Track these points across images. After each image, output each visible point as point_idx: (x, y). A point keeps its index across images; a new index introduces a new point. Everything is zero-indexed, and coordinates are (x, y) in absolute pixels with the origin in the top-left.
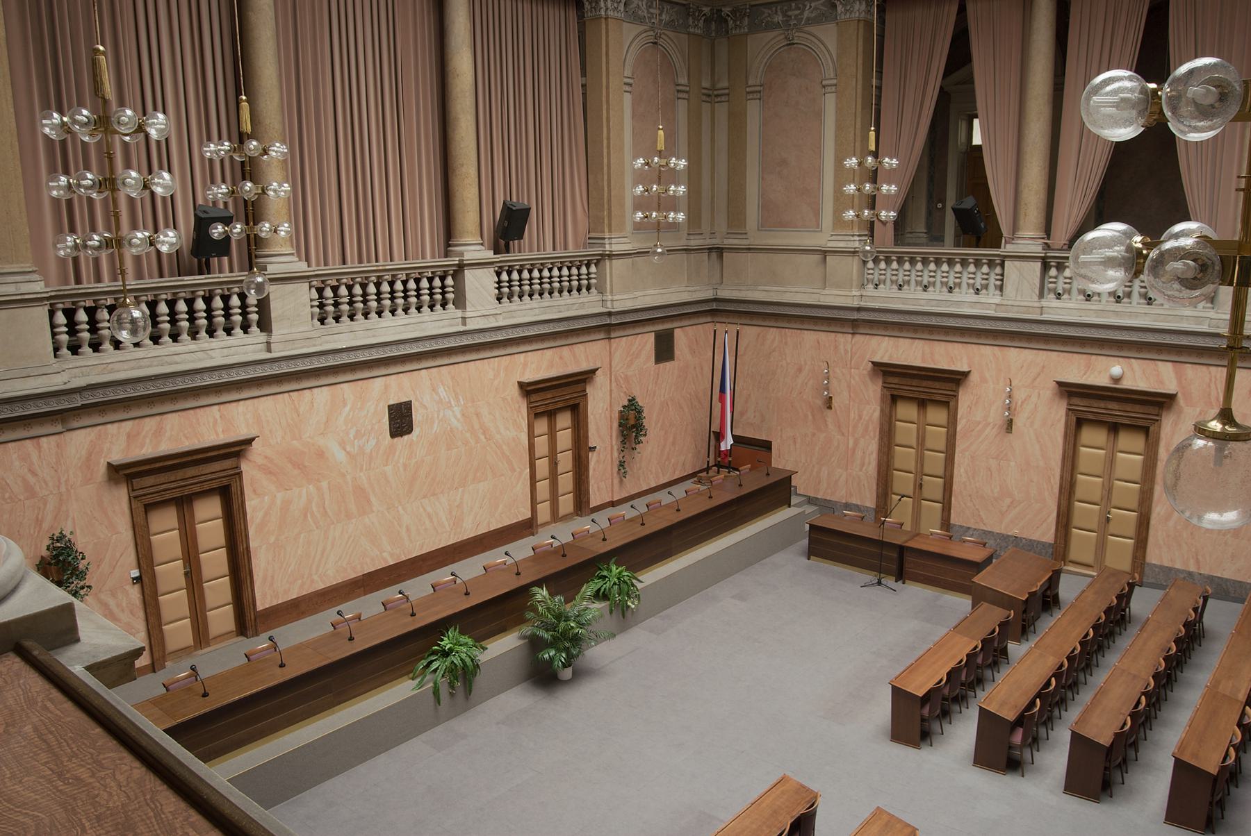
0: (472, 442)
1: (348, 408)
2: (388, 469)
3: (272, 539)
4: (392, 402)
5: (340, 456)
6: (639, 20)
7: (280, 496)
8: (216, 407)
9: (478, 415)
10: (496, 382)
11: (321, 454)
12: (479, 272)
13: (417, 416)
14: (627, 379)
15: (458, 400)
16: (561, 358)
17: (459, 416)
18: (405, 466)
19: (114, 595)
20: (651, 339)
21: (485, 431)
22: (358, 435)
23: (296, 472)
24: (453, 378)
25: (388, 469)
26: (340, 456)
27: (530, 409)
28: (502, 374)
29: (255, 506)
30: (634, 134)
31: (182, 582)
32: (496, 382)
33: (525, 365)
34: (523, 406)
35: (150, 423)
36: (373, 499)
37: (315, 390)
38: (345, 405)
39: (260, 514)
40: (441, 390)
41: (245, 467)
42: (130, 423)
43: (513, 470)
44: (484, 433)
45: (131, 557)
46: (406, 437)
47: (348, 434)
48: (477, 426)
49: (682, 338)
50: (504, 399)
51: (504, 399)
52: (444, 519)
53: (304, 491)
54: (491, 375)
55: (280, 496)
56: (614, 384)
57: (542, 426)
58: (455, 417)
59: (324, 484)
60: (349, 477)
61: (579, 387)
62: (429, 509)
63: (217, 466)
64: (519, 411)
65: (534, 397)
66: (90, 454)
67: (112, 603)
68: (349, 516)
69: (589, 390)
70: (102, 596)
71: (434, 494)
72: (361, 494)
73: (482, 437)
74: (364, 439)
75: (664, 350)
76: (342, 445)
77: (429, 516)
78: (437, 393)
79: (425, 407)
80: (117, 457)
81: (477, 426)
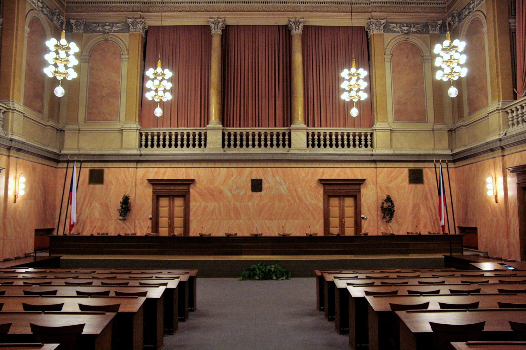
0: (292, 201)
1: (233, 178)
2: (250, 204)
3: (199, 218)
4: (254, 178)
5: (229, 194)
6: (399, 32)
7: (203, 204)
8: (184, 169)
9: (296, 191)
10: (306, 178)
11: (221, 192)
12: (299, 133)
13: (265, 185)
14: (388, 188)
15: (285, 182)
16: (345, 173)
17: (286, 189)
18: (257, 204)
19: (143, 222)
20: (406, 171)
21: (300, 198)
22: (237, 188)
23: (211, 196)
24: (283, 173)
25: (250, 204)
26: (229, 194)
27: (325, 192)
28: (310, 176)
29: (193, 205)
30: (393, 79)
31: (167, 225)
32: (306, 178)
33: (323, 173)
34: (321, 190)
35: (162, 170)
36: (242, 214)
37: (221, 169)
38: (232, 175)
39: (195, 208)
40: (277, 178)
41: (191, 190)
42: (156, 169)
43: (315, 218)
44: (299, 199)
45: (150, 211)
46: (259, 193)
47: (233, 187)
48: (295, 195)
49: (429, 174)
50: (310, 186)
51: (310, 186)
52: (275, 231)
53: (213, 204)
54: (304, 175)
55: (203, 204)
56: (379, 190)
57: (335, 202)
58: (284, 189)
59: (221, 204)
60: (232, 203)
61: (356, 187)
62: (268, 225)
63: (181, 188)
64: (319, 192)
65: (328, 188)
66: (143, 176)
67: (142, 224)
68: (230, 218)
69: (363, 190)
70: (140, 221)
71: (271, 219)
72: (236, 209)
73: (298, 200)
74: (240, 190)
75: (416, 177)
76: (230, 190)
77: (268, 227)
78: (275, 178)
79: (269, 183)
80: (150, 178)
81: (295, 195)
